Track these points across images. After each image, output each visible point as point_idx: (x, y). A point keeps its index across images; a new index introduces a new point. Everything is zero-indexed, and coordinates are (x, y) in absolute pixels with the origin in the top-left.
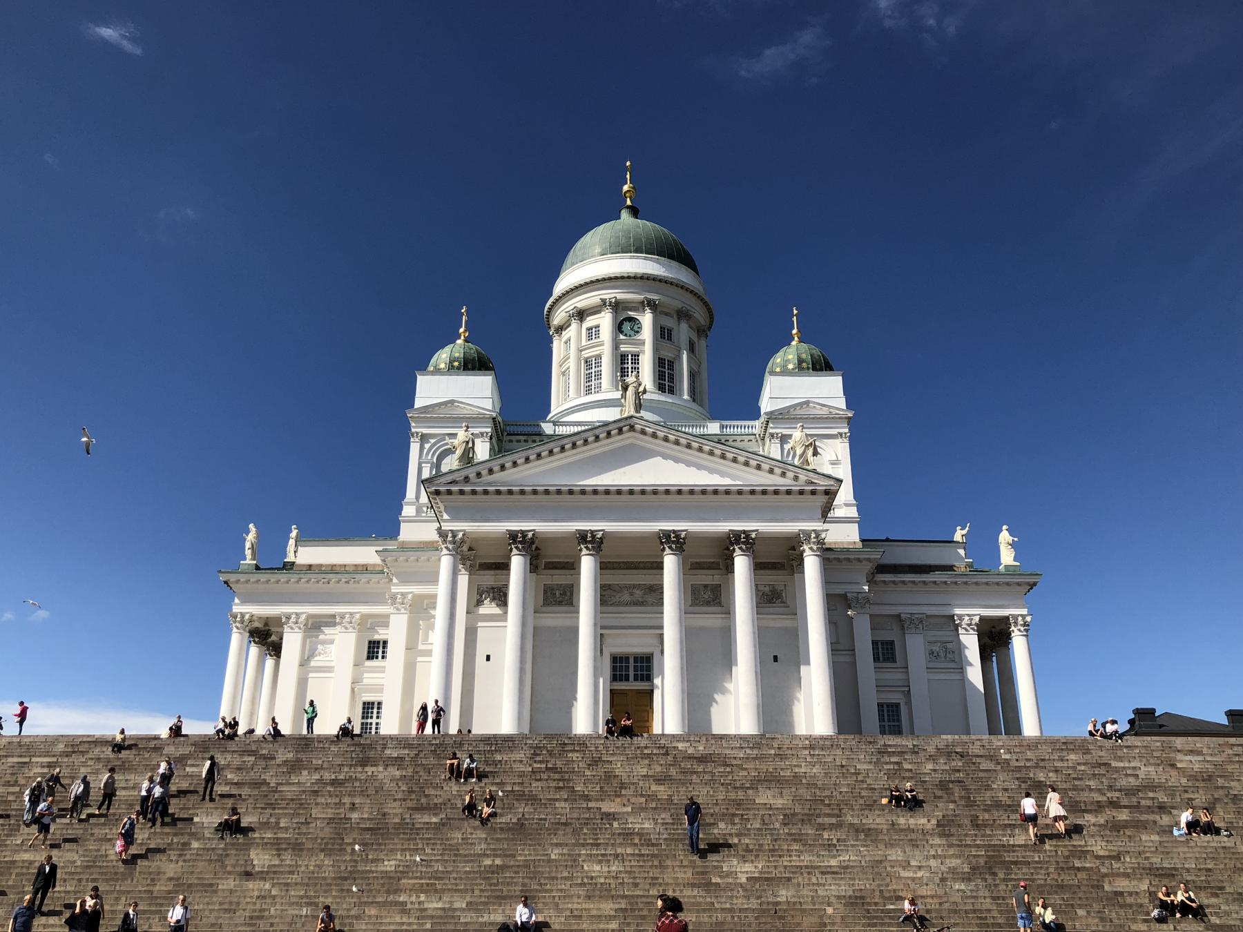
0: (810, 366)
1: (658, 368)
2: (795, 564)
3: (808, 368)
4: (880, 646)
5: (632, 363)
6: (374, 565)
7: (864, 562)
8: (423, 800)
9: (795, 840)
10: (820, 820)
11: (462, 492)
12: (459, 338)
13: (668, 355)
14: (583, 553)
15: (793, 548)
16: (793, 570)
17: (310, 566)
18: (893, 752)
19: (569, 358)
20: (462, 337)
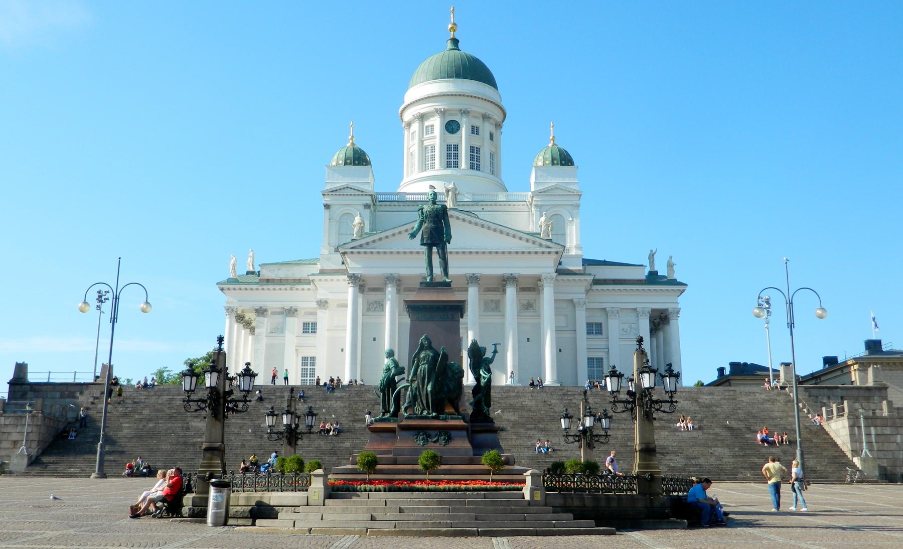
0: (559, 162)
2: (541, 288)
3: (557, 164)
4: (594, 326)
5: (454, 150)
6: (304, 279)
7: (585, 282)
8: (356, 417)
9: (515, 435)
10: (529, 426)
11: (359, 253)
12: (349, 142)
13: (476, 144)
15: (540, 280)
16: (539, 292)
17: (268, 280)
18: (570, 395)
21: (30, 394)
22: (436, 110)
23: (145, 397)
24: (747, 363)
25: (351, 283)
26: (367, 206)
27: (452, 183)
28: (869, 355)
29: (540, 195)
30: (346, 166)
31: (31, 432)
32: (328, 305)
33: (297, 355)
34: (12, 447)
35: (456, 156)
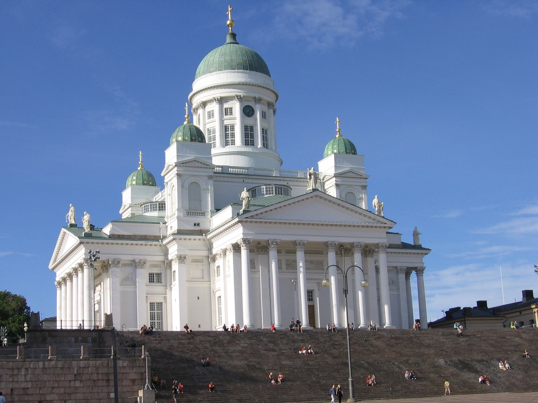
1: (262, 134)
6: (150, 236)
11: (251, 222)
12: (185, 120)
13: (266, 126)
14: (298, 249)
17: (119, 235)
19: (215, 121)
20: (187, 119)
21: (49, 339)
22: (237, 96)
23: (157, 342)
24: (460, 308)
25: (245, 246)
26: (210, 177)
27: (312, 168)
28: (527, 300)
29: (340, 177)
30: (192, 142)
31: (144, 372)
32: (186, 260)
33: (147, 302)
34: (132, 384)
35: (252, 136)
